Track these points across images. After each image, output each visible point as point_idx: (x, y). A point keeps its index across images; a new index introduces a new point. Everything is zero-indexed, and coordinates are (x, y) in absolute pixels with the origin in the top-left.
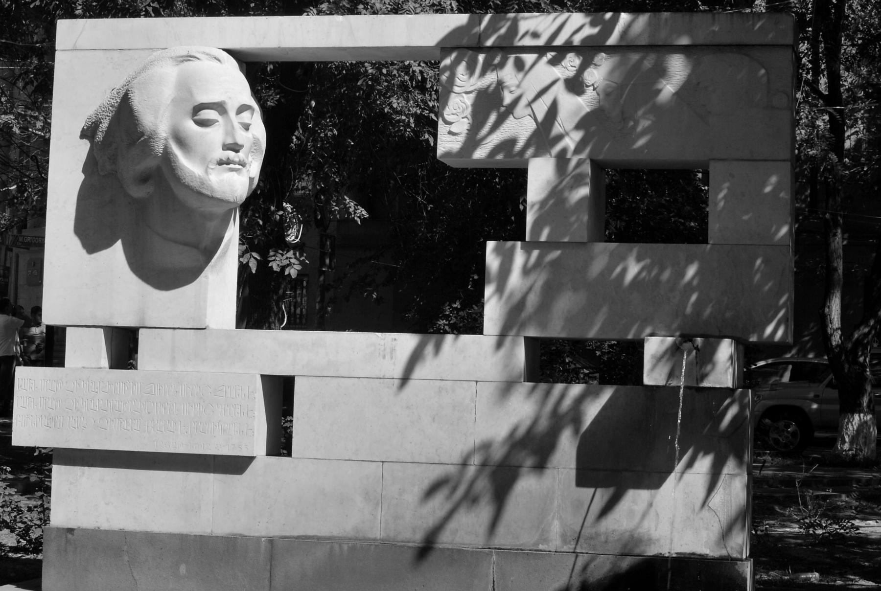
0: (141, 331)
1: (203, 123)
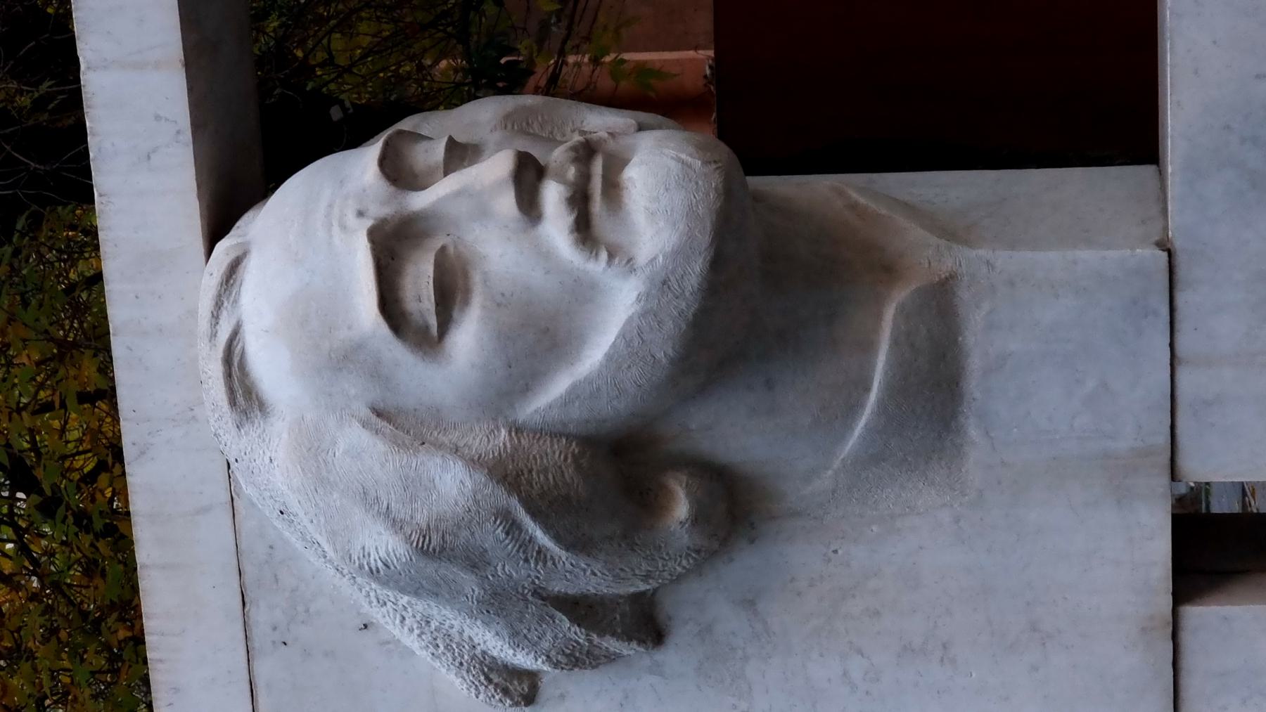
1: (450, 292)
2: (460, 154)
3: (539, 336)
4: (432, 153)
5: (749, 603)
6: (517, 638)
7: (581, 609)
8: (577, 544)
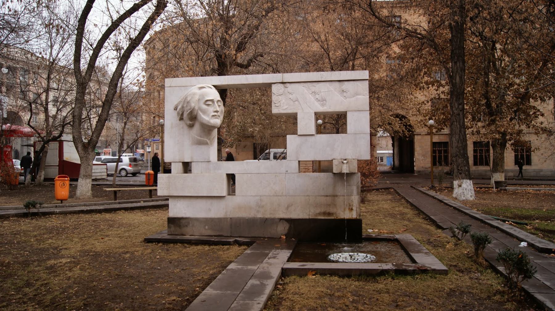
0: (193, 163)
1: (208, 105)
2: (219, 106)
3: (204, 112)
4: (219, 104)
5: (183, 128)
6: (180, 109)
7: (182, 115)
8: (188, 114)
